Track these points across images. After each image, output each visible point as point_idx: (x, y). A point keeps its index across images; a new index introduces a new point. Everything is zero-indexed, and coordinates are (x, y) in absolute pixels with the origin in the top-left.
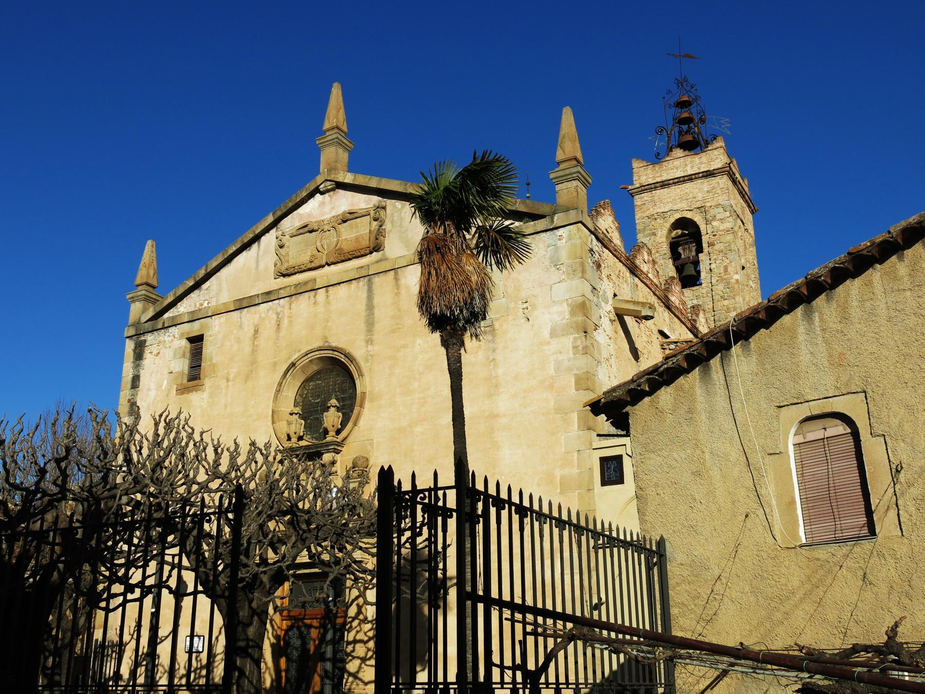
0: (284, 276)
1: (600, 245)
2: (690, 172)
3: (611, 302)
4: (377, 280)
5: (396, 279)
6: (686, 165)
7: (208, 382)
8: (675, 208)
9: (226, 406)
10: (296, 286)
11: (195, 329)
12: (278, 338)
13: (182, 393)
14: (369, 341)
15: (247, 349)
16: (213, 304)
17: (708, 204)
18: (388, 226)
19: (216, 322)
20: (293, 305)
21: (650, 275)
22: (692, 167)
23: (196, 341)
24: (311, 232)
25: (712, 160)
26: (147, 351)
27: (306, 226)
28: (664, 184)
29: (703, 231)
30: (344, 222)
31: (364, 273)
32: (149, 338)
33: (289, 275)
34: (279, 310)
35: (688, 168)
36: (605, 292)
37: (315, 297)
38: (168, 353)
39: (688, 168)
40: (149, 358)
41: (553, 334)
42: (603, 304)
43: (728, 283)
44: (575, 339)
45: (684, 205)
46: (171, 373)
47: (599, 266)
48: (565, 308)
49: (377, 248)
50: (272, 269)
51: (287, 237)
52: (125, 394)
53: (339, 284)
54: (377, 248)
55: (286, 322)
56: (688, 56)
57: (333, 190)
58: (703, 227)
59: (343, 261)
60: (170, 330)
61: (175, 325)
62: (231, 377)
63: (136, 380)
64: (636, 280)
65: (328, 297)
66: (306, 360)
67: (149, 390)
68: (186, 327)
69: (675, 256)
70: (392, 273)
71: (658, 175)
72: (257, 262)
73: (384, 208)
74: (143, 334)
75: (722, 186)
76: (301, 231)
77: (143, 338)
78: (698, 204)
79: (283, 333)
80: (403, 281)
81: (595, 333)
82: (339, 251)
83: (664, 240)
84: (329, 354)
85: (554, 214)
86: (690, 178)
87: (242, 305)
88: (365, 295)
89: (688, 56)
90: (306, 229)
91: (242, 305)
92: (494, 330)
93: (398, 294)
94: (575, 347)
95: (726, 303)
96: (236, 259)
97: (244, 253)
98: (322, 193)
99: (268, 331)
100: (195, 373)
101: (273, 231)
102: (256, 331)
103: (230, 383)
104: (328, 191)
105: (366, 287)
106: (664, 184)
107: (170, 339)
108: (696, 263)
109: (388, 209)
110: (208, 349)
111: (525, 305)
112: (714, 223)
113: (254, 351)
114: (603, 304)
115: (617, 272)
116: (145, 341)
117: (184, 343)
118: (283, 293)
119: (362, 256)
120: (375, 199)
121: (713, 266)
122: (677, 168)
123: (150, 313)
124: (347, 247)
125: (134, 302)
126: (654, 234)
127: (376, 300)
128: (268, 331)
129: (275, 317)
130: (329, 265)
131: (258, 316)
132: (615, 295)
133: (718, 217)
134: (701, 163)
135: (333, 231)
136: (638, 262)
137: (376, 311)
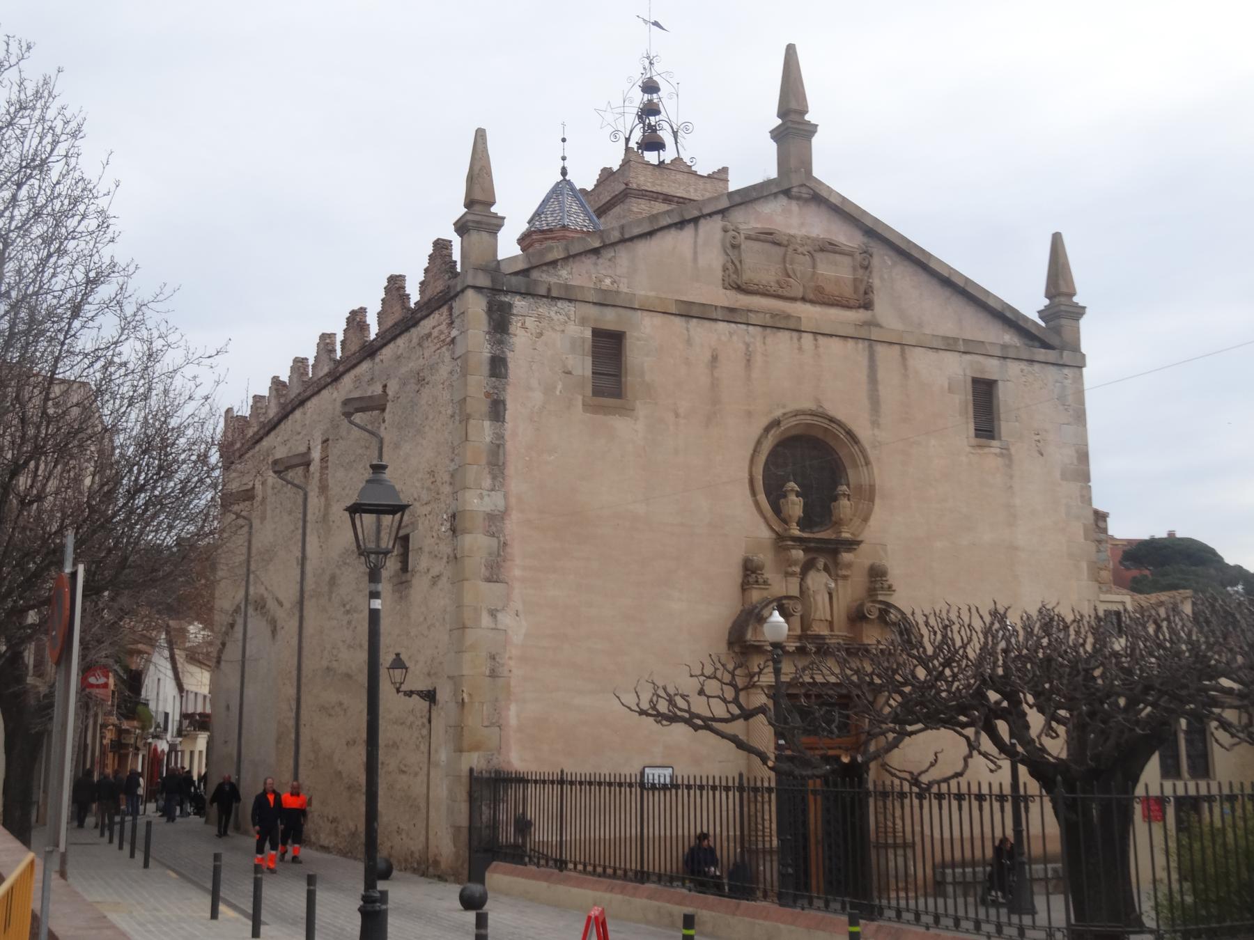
0: (739, 289)
4: (881, 350)
6: (690, 185)
10: (773, 316)
11: (609, 319)
14: (875, 424)
20: (769, 340)
26: (515, 326)
27: (771, 234)
30: (822, 250)
31: (863, 333)
32: (519, 304)
34: (747, 339)
37: (799, 339)
40: (520, 338)
41: (1064, 476)
46: (569, 373)
50: (719, 274)
53: (831, 336)
55: (758, 360)
56: (656, 24)
57: (806, 201)
61: (570, 300)
63: (498, 366)
65: (816, 347)
66: (793, 421)
68: (593, 311)
70: (898, 347)
74: (507, 292)
76: (762, 237)
77: (507, 299)
82: (819, 289)
89: (656, 24)
90: (768, 237)
97: (673, 232)
102: (715, 358)
104: (798, 198)
105: (867, 353)
111: (1037, 438)
113: (714, 385)
116: (510, 306)
119: (849, 307)
125: (478, 230)
127: (881, 375)
129: (742, 346)
130: (804, 299)
137: (880, 387)
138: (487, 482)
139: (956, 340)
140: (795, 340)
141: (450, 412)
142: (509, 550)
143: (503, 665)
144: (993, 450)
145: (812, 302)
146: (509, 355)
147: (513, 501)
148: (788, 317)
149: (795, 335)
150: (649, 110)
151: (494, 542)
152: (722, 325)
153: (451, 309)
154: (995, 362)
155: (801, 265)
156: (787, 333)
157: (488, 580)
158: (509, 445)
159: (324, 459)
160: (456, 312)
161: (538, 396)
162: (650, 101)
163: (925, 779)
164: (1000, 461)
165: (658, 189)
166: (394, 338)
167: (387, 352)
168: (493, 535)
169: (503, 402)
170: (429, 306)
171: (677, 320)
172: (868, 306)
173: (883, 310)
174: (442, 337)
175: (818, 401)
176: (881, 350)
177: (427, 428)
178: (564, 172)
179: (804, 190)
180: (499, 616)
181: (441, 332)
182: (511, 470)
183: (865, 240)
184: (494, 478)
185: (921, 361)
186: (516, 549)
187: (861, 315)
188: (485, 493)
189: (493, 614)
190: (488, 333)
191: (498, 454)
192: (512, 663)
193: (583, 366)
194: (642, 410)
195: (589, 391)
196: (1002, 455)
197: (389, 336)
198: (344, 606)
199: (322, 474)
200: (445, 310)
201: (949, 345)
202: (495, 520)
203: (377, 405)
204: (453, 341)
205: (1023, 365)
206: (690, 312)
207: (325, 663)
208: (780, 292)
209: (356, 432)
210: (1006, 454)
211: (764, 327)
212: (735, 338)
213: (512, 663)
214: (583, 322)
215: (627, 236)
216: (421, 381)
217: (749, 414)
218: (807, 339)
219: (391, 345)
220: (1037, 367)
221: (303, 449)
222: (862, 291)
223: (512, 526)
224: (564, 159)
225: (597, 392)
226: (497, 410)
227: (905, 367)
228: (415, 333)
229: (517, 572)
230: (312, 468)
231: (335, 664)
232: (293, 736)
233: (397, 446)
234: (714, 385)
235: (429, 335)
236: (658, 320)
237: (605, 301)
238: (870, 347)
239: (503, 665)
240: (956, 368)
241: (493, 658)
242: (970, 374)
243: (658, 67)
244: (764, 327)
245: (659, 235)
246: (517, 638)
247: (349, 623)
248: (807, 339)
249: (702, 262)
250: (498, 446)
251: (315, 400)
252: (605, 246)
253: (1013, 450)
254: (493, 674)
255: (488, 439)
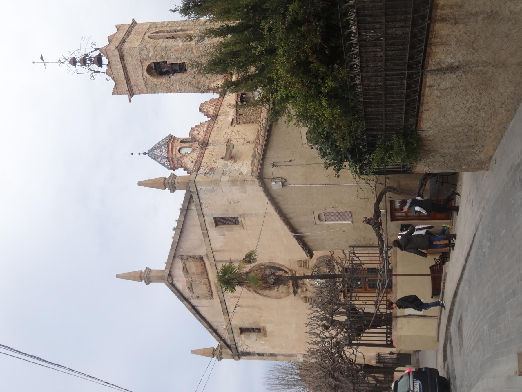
1: (201, 168)
2: (120, 66)
3: (226, 162)
4: (217, 258)
5: (217, 251)
6: (116, 68)
7: (262, 325)
8: (141, 74)
10: (218, 291)
11: (236, 331)
13: (267, 335)
16: (225, 324)
17: (139, 58)
18: (191, 254)
19: (234, 322)
21: (205, 130)
22: (117, 65)
23: (243, 330)
24: (191, 284)
25: (113, 55)
26: (246, 351)
28: (128, 79)
29: (155, 61)
32: (240, 350)
33: (212, 293)
35: (118, 67)
36: (223, 166)
38: (248, 342)
39: (118, 67)
40: (249, 350)
41: (245, 192)
42: (229, 168)
43: (184, 50)
44: (248, 184)
45: (140, 70)
47: (212, 169)
48: (234, 188)
49: (201, 258)
50: (209, 300)
51: (193, 295)
54: (201, 258)
56: (42, 58)
58: (152, 61)
59: (207, 272)
60: (236, 341)
62: (260, 315)
64: (210, 141)
67: (265, 349)
68: (236, 335)
69: (167, 73)
70: (214, 253)
71: (122, 82)
72: (205, 306)
73: (182, 256)
74: (238, 353)
75: (128, 51)
78: (139, 63)
80: (218, 249)
81: (244, 174)
82: (202, 274)
83: (159, 80)
85: (190, 191)
86: (124, 67)
87: (226, 312)
89: (42, 58)
90: (191, 287)
91: (226, 312)
92: (243, 214)
93: (224, 250)
94: (251, 184)
95: (195, 51)
96: (203, 315)
100: (257, 330)
101: (190, 300)
106: (128, 79)
107: (241, 341)
108: (172, 64)
109: (182, 254)
110: (246, 324)
112: (150, 55)
113: (248, 307)
114: (229, 168)
115: (210, 155)
117: (243, 335)
118: (221, 296)
119: (204, 263)
121: (174, 57)
122: (118, 73)
123: (228, 350)
124: (200, 270)
126: (156, 85)
129: (232, 299)
130: (208, 278)
132: (222, 158)
133: (147, 53)
134: (115, 60)
136: (201, 139)
139: (203, 233)
144: (243, 221)
145: (207, 275)
150: (84, 62)
154: (206, 218)
161: (266, 347)
162: (80, 62)
163: (374, 303)
164: (246, 219)
165: (125, 82)
173: (202, 251)
178: (145, 154)
179: (169, 279)
183: (177, 257)
185: (216, 245)
187: (205, 259)
196: (244, 218)
205: (203, 207)
208: (208, 284)
210: (244, 215)
220: (202, 201)
224: (140, 154)
227: (220, 251)
240: (214, 232)
242: (214, 228)
249: (207, 305)
253: (240, 213)
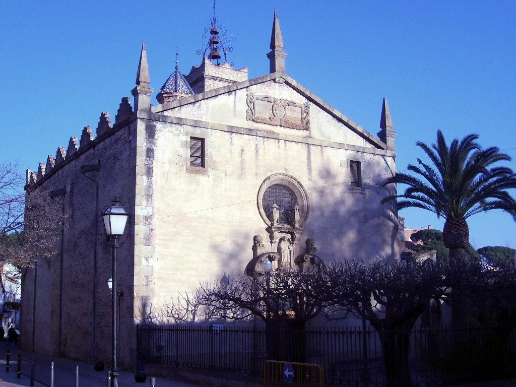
4: (312, 147)
9: (226, 190)
10: (268, 132)
11: (198, 133)
12: (257, 159)
15: (238, 160)
20: (266, 143)
30: (288, 105)
31: (305, 140)
49: (307, 129)
52: (141, 160)
55: (261, 151)
63: (150, 153)
68: (191, 129)
70: (320, 147)
79: (260, 157)
80: (325, 154)
82: (287, 122)
84: (289, 179)
88: (306, 153)
90: (266, 98)
98: (275, 82)
99: (249, 154)
102: (242, 150)
103: (228, 177)
113: (242, 162)
116: (155, 126)
120: (304, 100)
128: (249, 154)
129: (255, 146)
130: (280, 126)
131: (243, 141)
135: (283, 109)
137: (312, 164)
138: (145, 203)
140: (277, 143)
141: (128, 172)
142: (154, 232)
143: (151, 281)
146: (154, 148)
147: (156, 211)
148: (274, 133)
149: (277, 141)
150: (213, 42)
151: (147, 229)
152: (246, 136)
153: (129, 127)
155: (280, 112)
156: (273, 140)
157: (145, 245)
158: (154, 187)
159: (72, 191)
160: (132, 129)
166: (104, 140)
167: (100, 146)
168: (147, 226)
169: (152, 168)
170: (119, 126)
171: (226, 133)
172: (307, 129)
173: (315, 131)
174: (126, 140)
175: (286, 169)
176: (312, 147)
177: (118, 179)
180: (150, 260)
181: (125, 137)
182: (154, 197)
184: (148, 201)
185: (329, 152)
186: (156, 232)
187: (305, 133)
188: (144, 207)
189: (147, 259)
190: (146, 138)
191: (149, 191)
192: (155, 280)
193: (187, 153)
194: (211, 172)
195: (189, 164)
197: (100, 139)
198: (81, 255)
199: (71, 198)
200: (126, 128)
201: (341, 146)
202: (148, 218)
203: (96, 169)
204: (130, 141)
206: (231, 130)
207: (73, 280)
209: (86, 180)
211: (264, 137)
212: (251, 142)
213: (155, 280)
214: (187, 133)
215: (205, 98)
216: (116, 158)
217: (257, 174)
218: (282, 142)
219: (102, 143)
221: (62, 187)
222: (305, 121)
223: (155, 222)
225: (192, 164)
226: (149, 172)
228: (113, 138)
229: (157, 241)
230: (66, 196)
231: (77, 280)
232: (58, 311)
233: (105, 186)
234: (242, 162)
235: (120, 139)
236: (219, 133)
237: (196, 124)
238: (308, 147)
239: (151, 281)
241: (147, 277)
243: (218, 23)
244: (264, 137)
245: (219, 96)
246: (156, 269)
247: (83, 263)
248: (282, 142)
250: (150, 187)
251: (68, 166)
252: (196, 102)
254: (147, 284)
255: (145, 184)
